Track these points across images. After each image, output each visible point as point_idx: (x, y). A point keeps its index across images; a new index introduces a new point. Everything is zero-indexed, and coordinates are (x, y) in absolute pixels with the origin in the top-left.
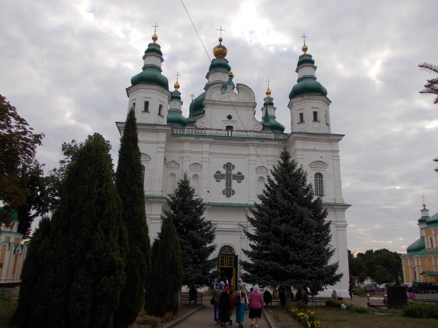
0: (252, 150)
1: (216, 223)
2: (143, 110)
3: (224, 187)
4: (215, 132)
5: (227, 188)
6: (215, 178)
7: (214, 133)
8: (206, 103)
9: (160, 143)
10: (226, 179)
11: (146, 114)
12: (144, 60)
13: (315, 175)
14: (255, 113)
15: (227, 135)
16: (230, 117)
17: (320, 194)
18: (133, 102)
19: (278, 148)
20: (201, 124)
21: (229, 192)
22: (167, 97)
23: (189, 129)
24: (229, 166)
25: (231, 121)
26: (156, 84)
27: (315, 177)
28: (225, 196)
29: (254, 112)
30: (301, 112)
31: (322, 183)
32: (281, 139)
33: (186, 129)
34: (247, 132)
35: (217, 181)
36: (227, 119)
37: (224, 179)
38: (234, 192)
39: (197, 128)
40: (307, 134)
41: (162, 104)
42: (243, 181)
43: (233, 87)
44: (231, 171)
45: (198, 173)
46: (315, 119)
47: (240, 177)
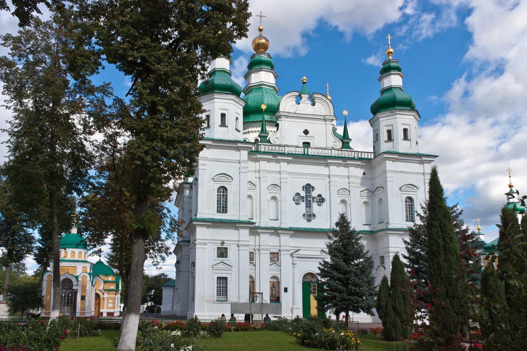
0: (334, 170)
1: (298, 249)
2: (220, 125)
3: (304, 211)
4: (294, 149)
6: (294, 200)
7: (292, 150)
9: (243, 162)
15: (303, 153)
16: (306, 132)
19: (361, 168)
20: (276, 140)
24: (308, 188)
26: (229, 93)
31: (412, 208)
32: (364, 159)
35: (296, 204)
36: (304, 135)
38: (314, 216)
39: (272, 145)
41: (238, 116)
42: (324, 204)
44: (310, 193)
45: (277, 196)
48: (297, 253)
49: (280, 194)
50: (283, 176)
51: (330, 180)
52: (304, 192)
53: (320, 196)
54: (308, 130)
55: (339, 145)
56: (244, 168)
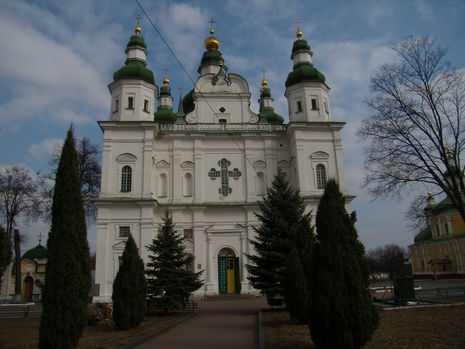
5: (223, 187)
6: (209, 176)
8: (196, 96)
11: (131, 112)
12: (127, 54)
13: (317, 167)
14: (249, 104)
16: (222, 110)
17: (323, 186)
18: (116, 99)
21: (226, 190)
22: (153, 92)
23: (178, 125)
24: (224, 163)
25: (225, 114)
27: (317, 169)
28: (221, 195)
29: (249, 103)
30: (298, 100)
33: (174, 125)
34: (242, 124)
35: (212, 179)
36: (220, 112)
37: (219, 176)
38: (231, 190)
39: (187, 124)
40: (306, 124)
41: (148, 99)
42: (241, 178)
43: (224, 78)
44: (226, 168)
45: (191, 172)
46: (314, 107)
47: (237, 174)
48: (211, 228)
49: (194, 170)
50: (196, 152)
52: (220, 167)
53: (236, 169)
55: (256, 120)
56: (148, 146)
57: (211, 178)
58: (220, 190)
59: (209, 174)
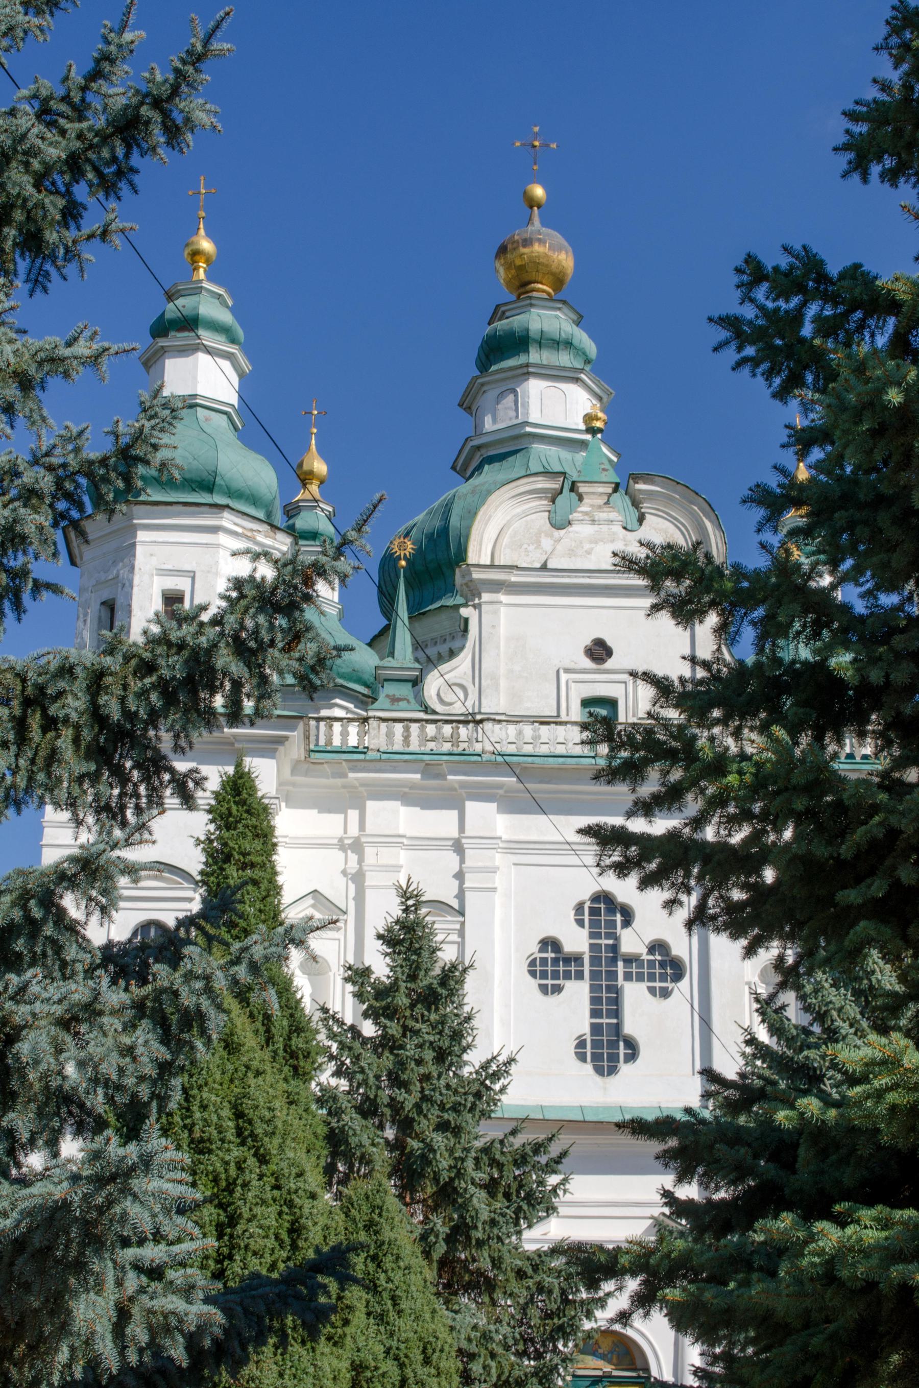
3: (583, 1024)
4: (528, 730)
5: (596, 1029)
6: (533, 974)
10: (595, 975)
18: (106, 595)
28: (588, 1068)
35: (544, 989)
36: (588, 663)
37: (580, 976)
43: (610, 490)
51: (462, 861)
52: (584, 933)
54: (609, 643)
57: (540, 985)
58: (581, 1044)
59: (533, 963)
